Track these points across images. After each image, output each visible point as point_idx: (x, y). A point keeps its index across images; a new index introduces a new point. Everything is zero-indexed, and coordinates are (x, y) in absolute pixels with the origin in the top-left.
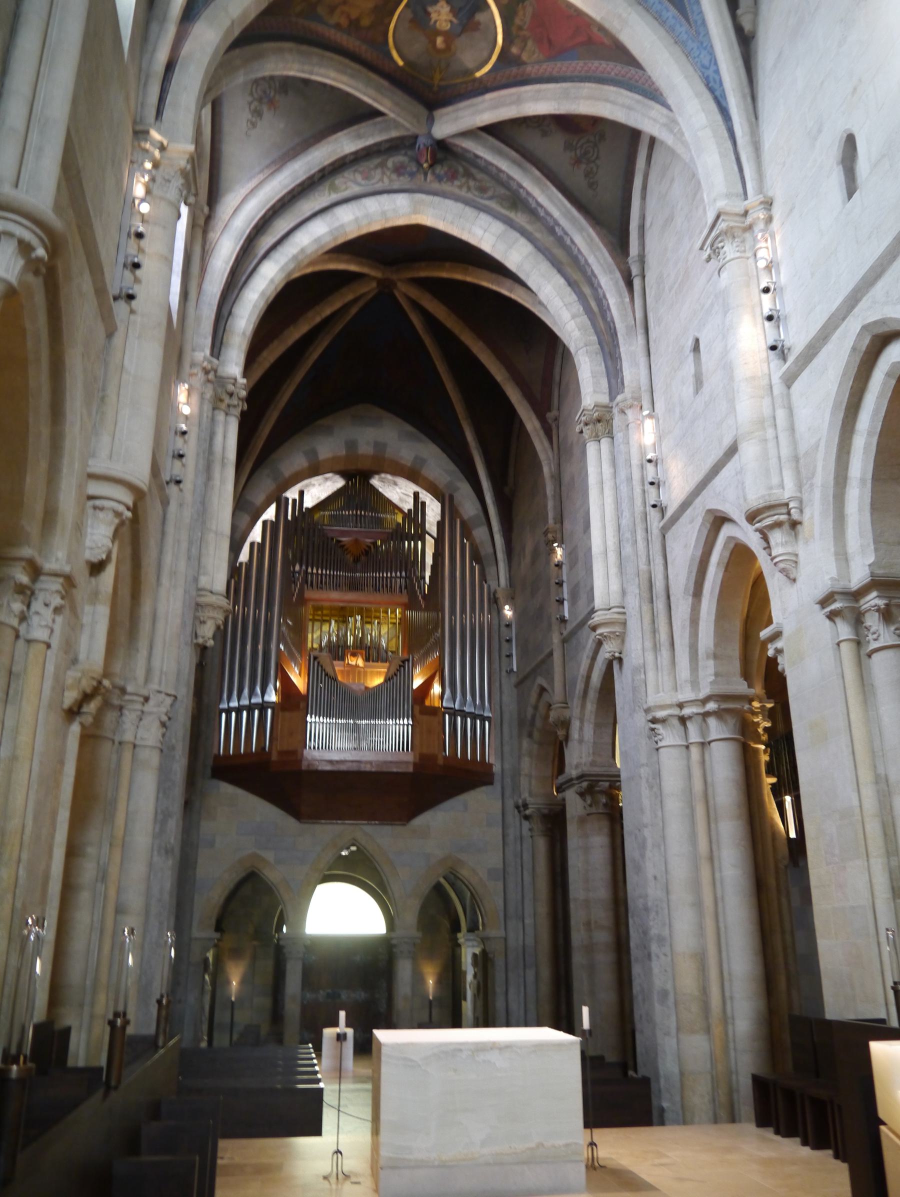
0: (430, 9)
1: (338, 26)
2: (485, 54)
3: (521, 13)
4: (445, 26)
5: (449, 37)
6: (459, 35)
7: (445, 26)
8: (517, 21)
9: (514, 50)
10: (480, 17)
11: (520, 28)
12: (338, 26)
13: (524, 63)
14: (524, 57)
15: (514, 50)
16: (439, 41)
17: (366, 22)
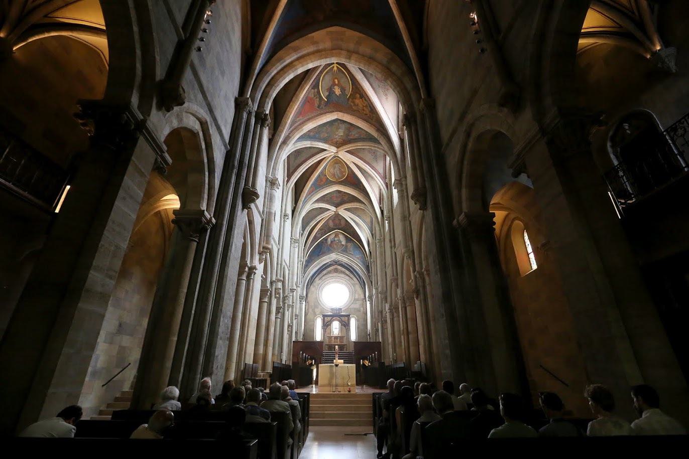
0: (341, 93)
1: (365, 100)
2: (323, 83)
3: (318, 102)
4: (336, 87)
5: (334, 84)
6: (332, 85)
7: (336, 87)
8: (318, 99)
9: (316, 90)
10: (327, 94)
11: (316, 98)
12: (365, 100)
13: (312, 89)
14: (313, 90)
15: (316, 90)
16: (337, 83)
17: (358, 96)
